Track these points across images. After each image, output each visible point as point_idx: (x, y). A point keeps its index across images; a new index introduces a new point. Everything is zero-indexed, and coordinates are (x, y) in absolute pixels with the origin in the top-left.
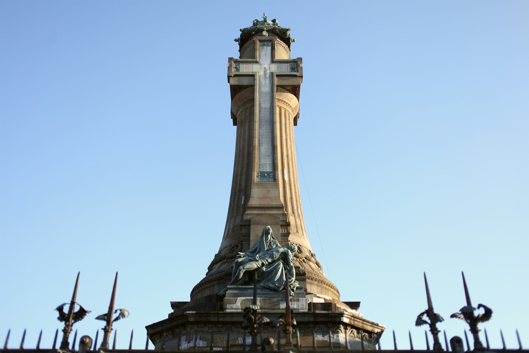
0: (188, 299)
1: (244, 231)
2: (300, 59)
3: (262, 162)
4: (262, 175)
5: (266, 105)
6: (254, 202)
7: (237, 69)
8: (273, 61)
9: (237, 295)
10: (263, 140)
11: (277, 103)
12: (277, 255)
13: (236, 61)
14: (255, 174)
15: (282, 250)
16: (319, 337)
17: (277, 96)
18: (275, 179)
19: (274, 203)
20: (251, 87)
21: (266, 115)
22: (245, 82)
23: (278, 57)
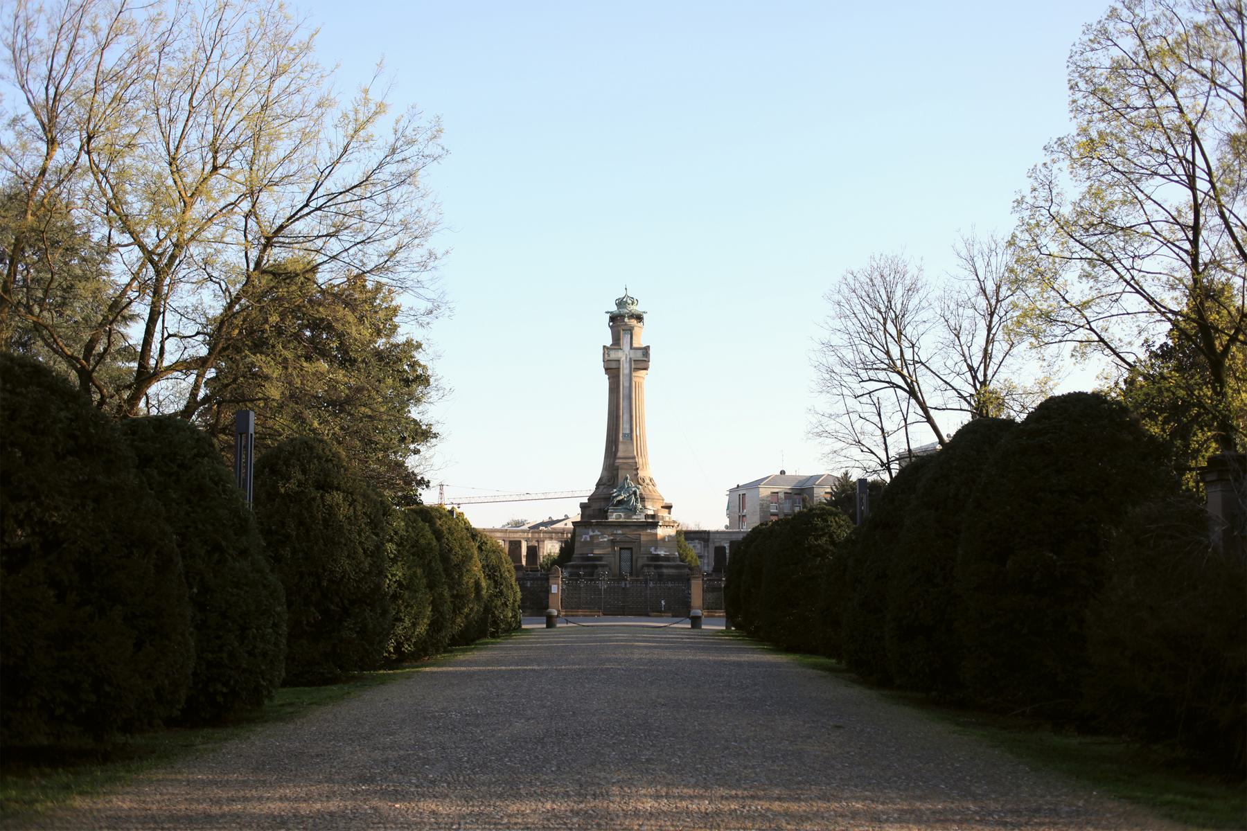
0: (587, 501)
1: (615, 472)
2: (649, 347)
3: (625, 426)
4: (624, 435)
5: (627, 384)
6: (620, 454)
7: (609, 355)
8: (631, 348)
9: (613, 512)
10: (625, 411)
11: (634, 379)
12: (631, 492)
13: (608, 348)
14: (621, 435)
15: (634, 489)
16: (649, 531)
17: (634, 374)
18: (631, 439)
19: (631, 455)
20: (618, 369)
21: (627, 391)
22: (614, 365)
23: (634, 345)
